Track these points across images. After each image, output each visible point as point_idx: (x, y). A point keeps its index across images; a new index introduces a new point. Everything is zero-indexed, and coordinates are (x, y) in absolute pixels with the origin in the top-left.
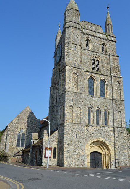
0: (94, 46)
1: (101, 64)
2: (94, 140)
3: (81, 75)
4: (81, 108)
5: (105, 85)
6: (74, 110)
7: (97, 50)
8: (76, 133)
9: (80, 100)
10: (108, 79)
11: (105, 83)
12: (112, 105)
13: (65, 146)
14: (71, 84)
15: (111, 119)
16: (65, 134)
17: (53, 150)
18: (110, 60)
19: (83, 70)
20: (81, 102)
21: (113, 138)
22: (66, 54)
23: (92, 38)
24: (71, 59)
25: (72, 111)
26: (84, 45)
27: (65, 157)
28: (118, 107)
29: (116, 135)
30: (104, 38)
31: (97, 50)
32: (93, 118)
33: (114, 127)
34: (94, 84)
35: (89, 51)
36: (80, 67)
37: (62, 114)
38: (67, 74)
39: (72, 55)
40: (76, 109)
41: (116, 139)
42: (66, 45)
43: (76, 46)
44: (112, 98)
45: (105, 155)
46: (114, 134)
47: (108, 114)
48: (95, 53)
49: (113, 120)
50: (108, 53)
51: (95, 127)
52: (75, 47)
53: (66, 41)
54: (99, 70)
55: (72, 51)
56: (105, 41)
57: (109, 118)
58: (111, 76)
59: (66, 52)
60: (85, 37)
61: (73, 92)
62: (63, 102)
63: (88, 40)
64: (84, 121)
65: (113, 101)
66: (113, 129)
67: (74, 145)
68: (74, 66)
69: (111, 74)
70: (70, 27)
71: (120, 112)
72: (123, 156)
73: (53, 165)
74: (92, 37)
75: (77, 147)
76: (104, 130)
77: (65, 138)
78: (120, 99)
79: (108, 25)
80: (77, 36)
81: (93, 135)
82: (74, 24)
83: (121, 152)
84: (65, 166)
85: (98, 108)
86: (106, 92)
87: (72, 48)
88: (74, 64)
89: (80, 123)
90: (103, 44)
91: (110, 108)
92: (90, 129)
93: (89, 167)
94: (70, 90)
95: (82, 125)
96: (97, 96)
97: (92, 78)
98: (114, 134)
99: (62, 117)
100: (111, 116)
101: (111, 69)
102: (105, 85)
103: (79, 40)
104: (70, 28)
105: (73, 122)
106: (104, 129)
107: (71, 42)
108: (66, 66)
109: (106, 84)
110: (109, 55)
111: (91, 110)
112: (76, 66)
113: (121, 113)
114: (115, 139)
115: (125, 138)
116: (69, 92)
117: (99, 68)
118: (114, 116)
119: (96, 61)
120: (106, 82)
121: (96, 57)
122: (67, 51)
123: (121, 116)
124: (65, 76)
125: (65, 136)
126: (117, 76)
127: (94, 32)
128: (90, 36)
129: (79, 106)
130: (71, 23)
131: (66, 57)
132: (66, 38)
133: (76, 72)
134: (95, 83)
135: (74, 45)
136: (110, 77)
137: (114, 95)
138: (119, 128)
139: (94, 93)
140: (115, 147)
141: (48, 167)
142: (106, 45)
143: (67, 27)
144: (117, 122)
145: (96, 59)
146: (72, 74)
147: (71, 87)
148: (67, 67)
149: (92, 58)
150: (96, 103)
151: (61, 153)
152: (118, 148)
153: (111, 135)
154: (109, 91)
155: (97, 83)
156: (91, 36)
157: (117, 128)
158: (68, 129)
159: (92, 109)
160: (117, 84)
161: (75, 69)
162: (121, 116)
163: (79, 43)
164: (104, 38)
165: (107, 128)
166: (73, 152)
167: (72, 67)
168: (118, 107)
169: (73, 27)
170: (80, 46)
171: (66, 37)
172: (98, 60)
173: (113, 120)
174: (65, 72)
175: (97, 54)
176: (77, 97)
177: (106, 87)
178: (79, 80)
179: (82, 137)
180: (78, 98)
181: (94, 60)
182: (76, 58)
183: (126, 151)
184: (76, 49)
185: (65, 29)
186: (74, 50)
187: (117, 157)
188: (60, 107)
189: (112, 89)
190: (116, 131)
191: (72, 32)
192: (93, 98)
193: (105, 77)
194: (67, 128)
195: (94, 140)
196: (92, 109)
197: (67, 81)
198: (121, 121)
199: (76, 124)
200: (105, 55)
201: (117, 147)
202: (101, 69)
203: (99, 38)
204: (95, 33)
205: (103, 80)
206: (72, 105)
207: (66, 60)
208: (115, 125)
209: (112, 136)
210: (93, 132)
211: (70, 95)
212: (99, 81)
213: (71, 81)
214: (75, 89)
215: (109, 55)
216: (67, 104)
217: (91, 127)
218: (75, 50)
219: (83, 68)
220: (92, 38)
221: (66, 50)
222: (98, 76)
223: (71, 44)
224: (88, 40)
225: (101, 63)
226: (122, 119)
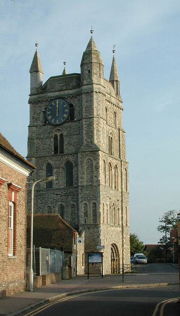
21: (121, 240)
22: (95, 131)
33: (122, 228)
37: (90, 212)
40: (105, 208)
41: (124, 240)
46: (123, 235)
49: (122, 218)
53: (95, 113)
59: (95, 130)
65: (122, 195)
66: (121, 229)
69: (120, 158)
79: (117, 81)
91: (120, 202)
98: (123, 235)
114: (123, 241)
128: (108, 103)
131: (95, 137)
132: (95, 109)
143: (96, 92)
173: (122, 218)
207: (96, 142)
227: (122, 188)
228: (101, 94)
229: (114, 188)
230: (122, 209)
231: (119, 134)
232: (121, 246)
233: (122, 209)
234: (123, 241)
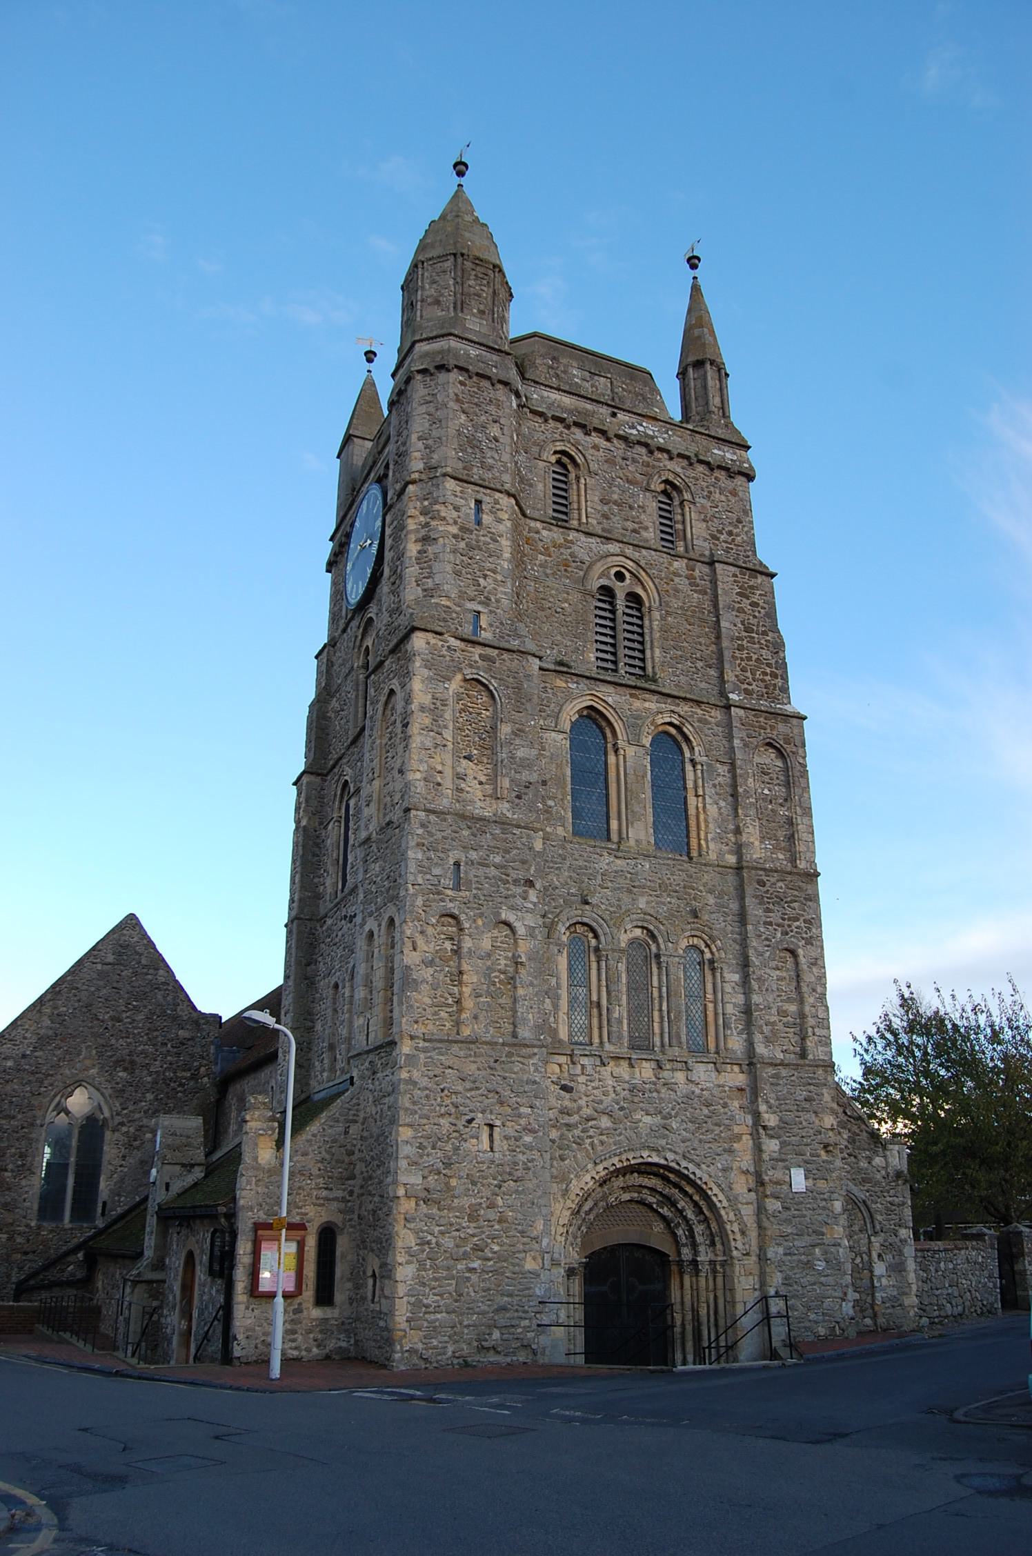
0: (603, 501)
1: (654, 622)
2: (615, 1160)
3: (520, 697)
4: (521, 931)
5: (689, 767)
6: (467, 943)
7: (630, 525)
8: (483, 1112)
9: (514, 875)
10: (706, 722)
11: (687, 754)
12: (734, 906)
13: (407, 1206)
14: (444, 761)
15: (730, 1009)
16: (404, 1118)
17: (311, 1242)
18: (716, 596)
19: (536, 663)
20: (519, 890)
22: (412, 549)
23: (591, 448)
24: (451, 586)
25: (457, 952)
26: (542, 488)
27: (401, 1290)
28: (775, 917)
29: (771, 1120)
30: (675, 452)
31: (630, 525)
32: (604, 1002)
34: (612, 759)
35: (572, 535)
36: (515, 644)
37: (379, 973)
38: (417, 685)
39: (459, 558)
41: (771, 1146)
42: (411, 487)
43: (482, 494)
44: (732, 859)
45: (694, 1263)
46: (757, 1115)
47: (713, 970)
48: (613, 548)
50: (703, 546)
51: (623, 1070)
52: (478, 502)
53: (416, 465)
54: (643, 660)
55: (454, 530)
56: (677, 466)
57: (715, 1002)
58: (728, 707)
60: (552, 439)
61: (463, 817)
62: (392, 891)
63: (565, 460)
64: (545, 1027)
67: (466, 1202)
68: (467, 630)
69: (723, 694)
70: (441, 367)
71: (793, 953)
72: (820, 1265)
73: (315, 1350)
74: (596, 439)
75: (492, 1215)
76: (683, 1088)
77: (406, 1150)
78: (789, 868)
80: (494, 431)
81: (605, 1122)
82: (473, 352)
83: (808, 1240)
84: (400, 1360)
85: (638, 932)
86: (692, 811)
87: (457, 509)
88: (470, 616)
89: (510, 1040)
90: (671, 489)
91: (723, 925)
92: (582, 1079)
93: (580, 1360)
94: (444, 803)
95: (524, 1051)
96: (632, 842)
97: (593, 717)
99: (379, 998)
100: (728, 988)
101: (727, 655)
102: (689, 767)
103: (506, 457)
104: (442, 377)
105: (466, 1032)
106: (680, 1077)
107: (449, 469)
108: (414, 629)
109: (692, 760)
110: (711, 563)
111: (593, 942)
112: (486, 636)
113: (802, 960)
114: (758, 1149)
115: (832, 1137)
116: (432, 818)
117: (643, 652)
118: (754, 984)
119: (621, 603)
120: (692, 749)
121: (620, 576)
122: (423, 532)
123: (798, 987)
124: (408, 700)
125: (405, 1133)
126: (764, 704)
127: (604, 411)
128: (578, 434)
129: (505, 915)
130: (453, 343)
131: (412, 571)
133: (484, 676)
134: (616, 751)
135: (470, 489)
136: (717, 714)
137: (752, 833)
138: (784, 1072)
139: (614, 824)
140: (760, 1210)
141: (276, 1371)
142: (687, 496)
143: (424, 372)
144: (773, 1024)
145: (621, 590)
146: (455, 685)
147: (448, 782)
148: (419, 641)
149: (595, 583)
150: (626, 898)
151: (373, 1263)
152: (786, 1214)
153: (732, 1118)
154: (713, 810)
155: (631, 751)
156: (587, 434)
157: (771, 1071)
158: (424, 1082)
159: (596, 936)
160: (769, 758)
161: (478, 650)
162: (798, 987)
163: (507, 478)
164: (675, 452)
165: (703, 1073)
166: (466, 1256)
167: (457, 643)
168: (775, 917)
169: (461, 369)
170: (509, 494)
171: (414, 437)
172: (633, 598)
173: (748, 1011)
174: (406, 675)
175: (629, 551)
176: (492, 850)
177: (690, 784)
178: (505, 730)
179: (528, 1139)
180: (498, 859)
181: (607, 591)
182: (485, 577)
183: (839, 1231)
184: (487, 519)
185: (408, 380)
186: (472, 526)
187: (776, 1280)
188: (371, 924)
189: (734, 795)
190: (766, 1090)
191: (458, 400)
192: (605, 862)
193: (684, 708)
194: (416, 1075)
195: (615, 1160)
196: (596, 936)
197: (418, 738)
198: (802, 1015)
199: (485, 1049)
200: (679, 565)
201: (773, 1205)
202: (656, 655)
203: (643, 450)
204: (614, 415)
205: (673, 731)
206: (452, 907)
208: (761, 1049)
209: (736, 1129)
210: (607, 1100)
211: (439, 835)
212: (647, 741)
213: (448, 734)
214: (479, 794)
215: (711, 563)
216: (419, 901)
217: (589, 1070)
218: (479, 523)
219: (531, 646)
220: (596, 447)
221: (411, 525)
222: (637, 704)
223: (450, 484)
224: (565, 460)
225: (656, 615)
226: (807, 1009)
227: (739, 850)
228: (455, 376)
229: (641, 833)
230: (745, 964)
231: (714, 582)
232: (741, 1185)
233: (745, 964)
234: (758, 1149)
